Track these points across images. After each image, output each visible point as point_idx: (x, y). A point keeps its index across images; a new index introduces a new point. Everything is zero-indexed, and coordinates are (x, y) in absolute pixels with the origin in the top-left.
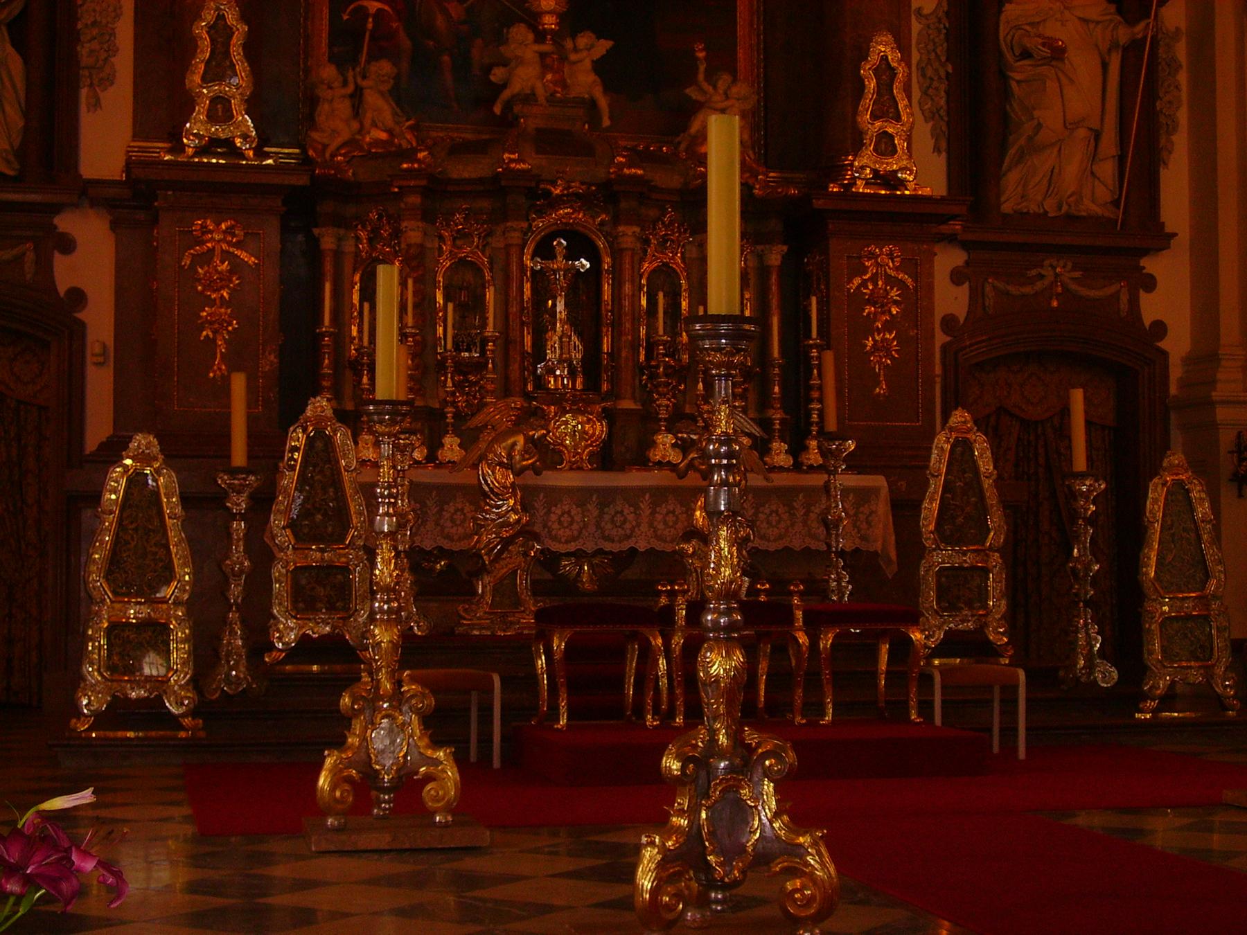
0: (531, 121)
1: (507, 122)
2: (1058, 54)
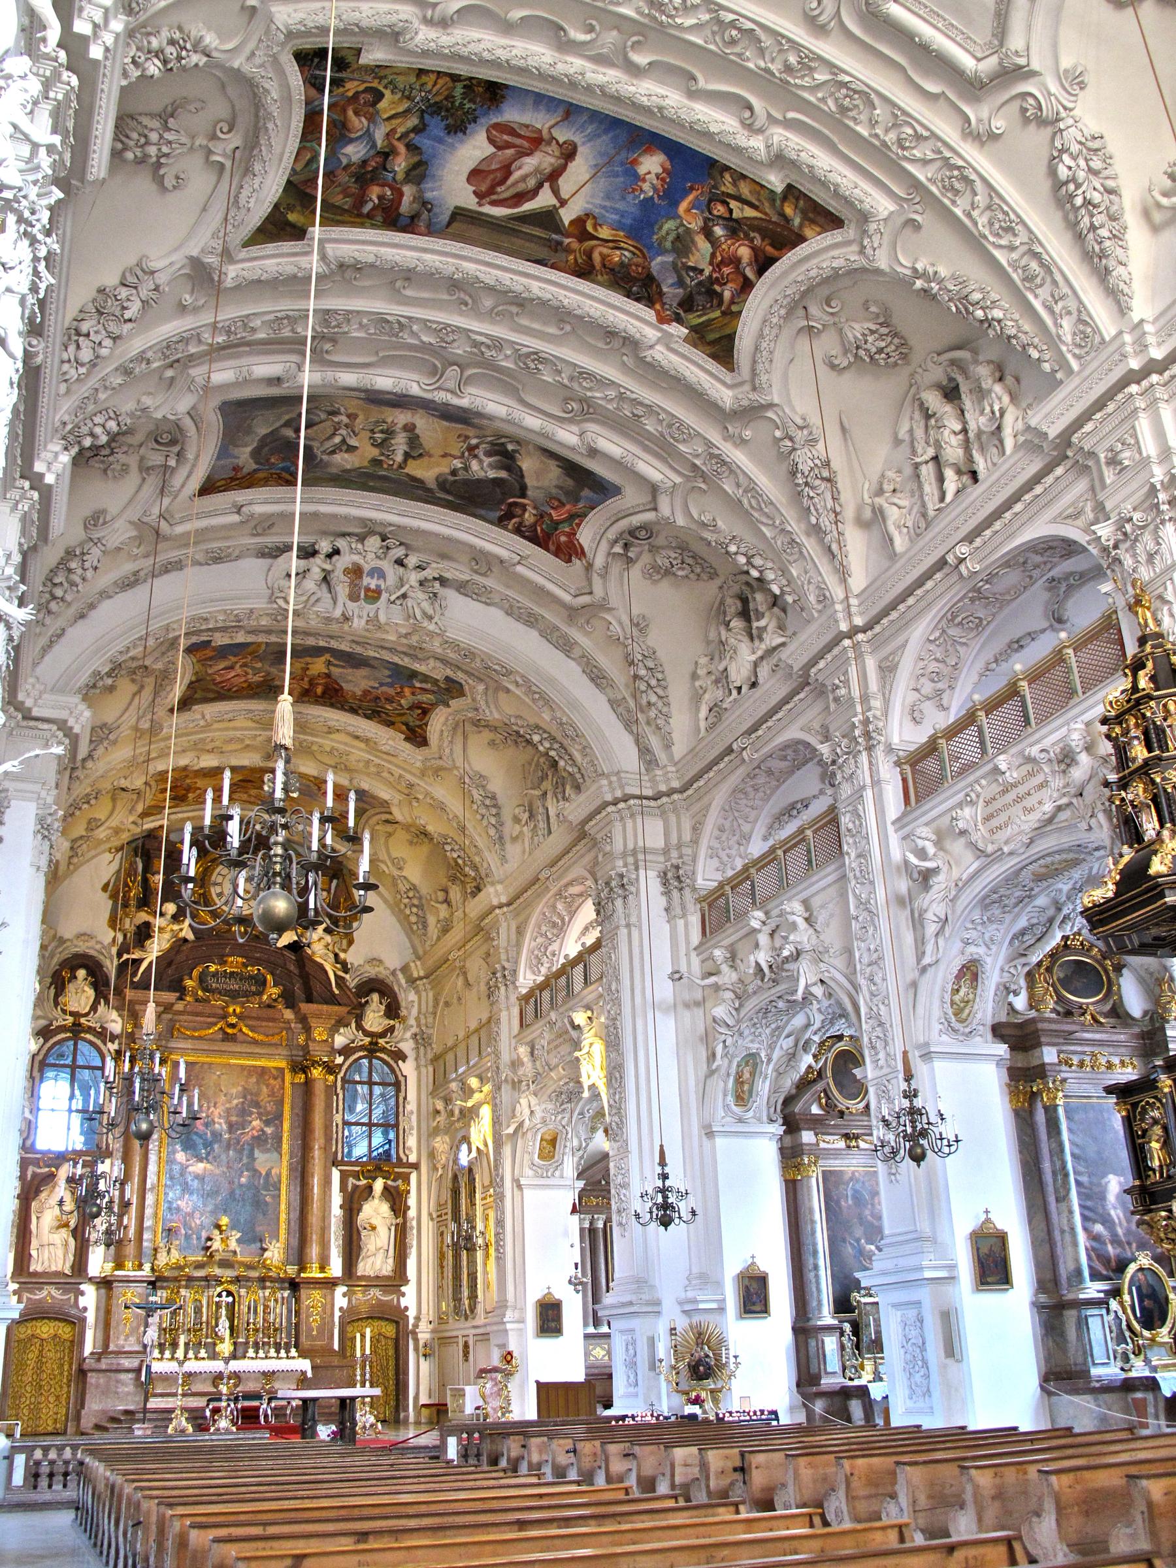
0: (217, 1257)
1: (211, 1256)
2: (374, 1228)
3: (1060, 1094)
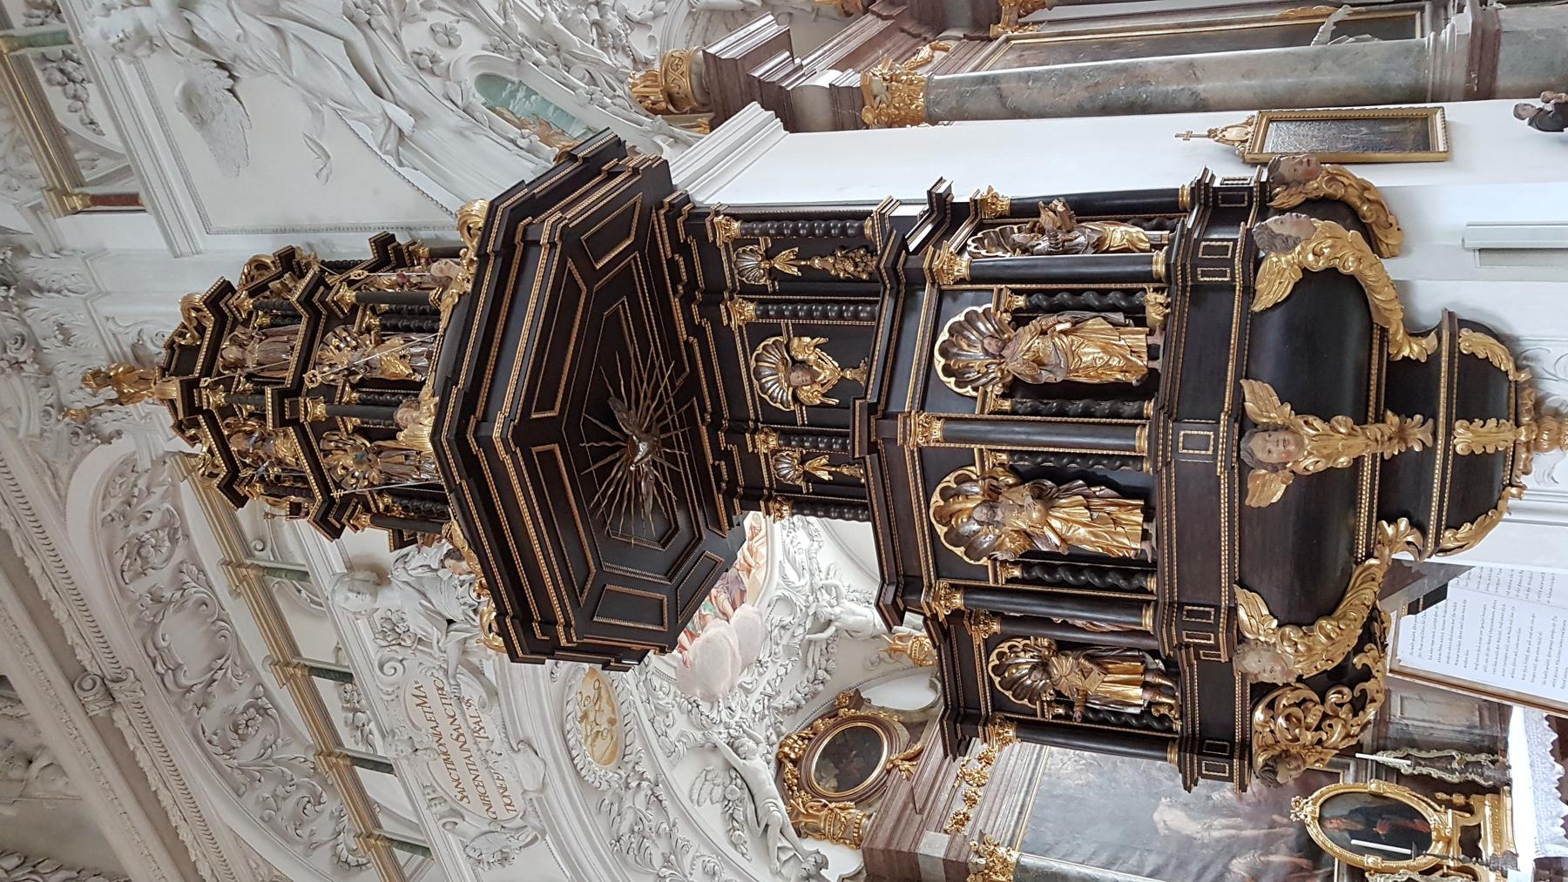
3: (1002, 851)
